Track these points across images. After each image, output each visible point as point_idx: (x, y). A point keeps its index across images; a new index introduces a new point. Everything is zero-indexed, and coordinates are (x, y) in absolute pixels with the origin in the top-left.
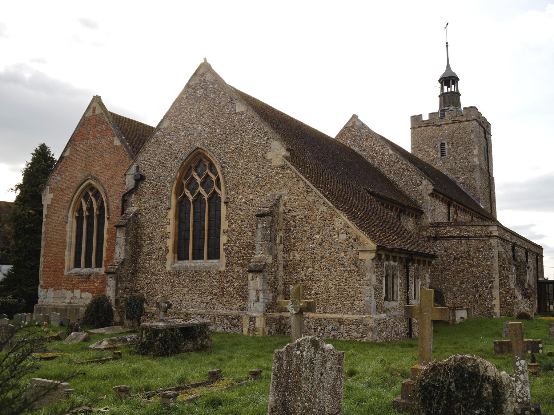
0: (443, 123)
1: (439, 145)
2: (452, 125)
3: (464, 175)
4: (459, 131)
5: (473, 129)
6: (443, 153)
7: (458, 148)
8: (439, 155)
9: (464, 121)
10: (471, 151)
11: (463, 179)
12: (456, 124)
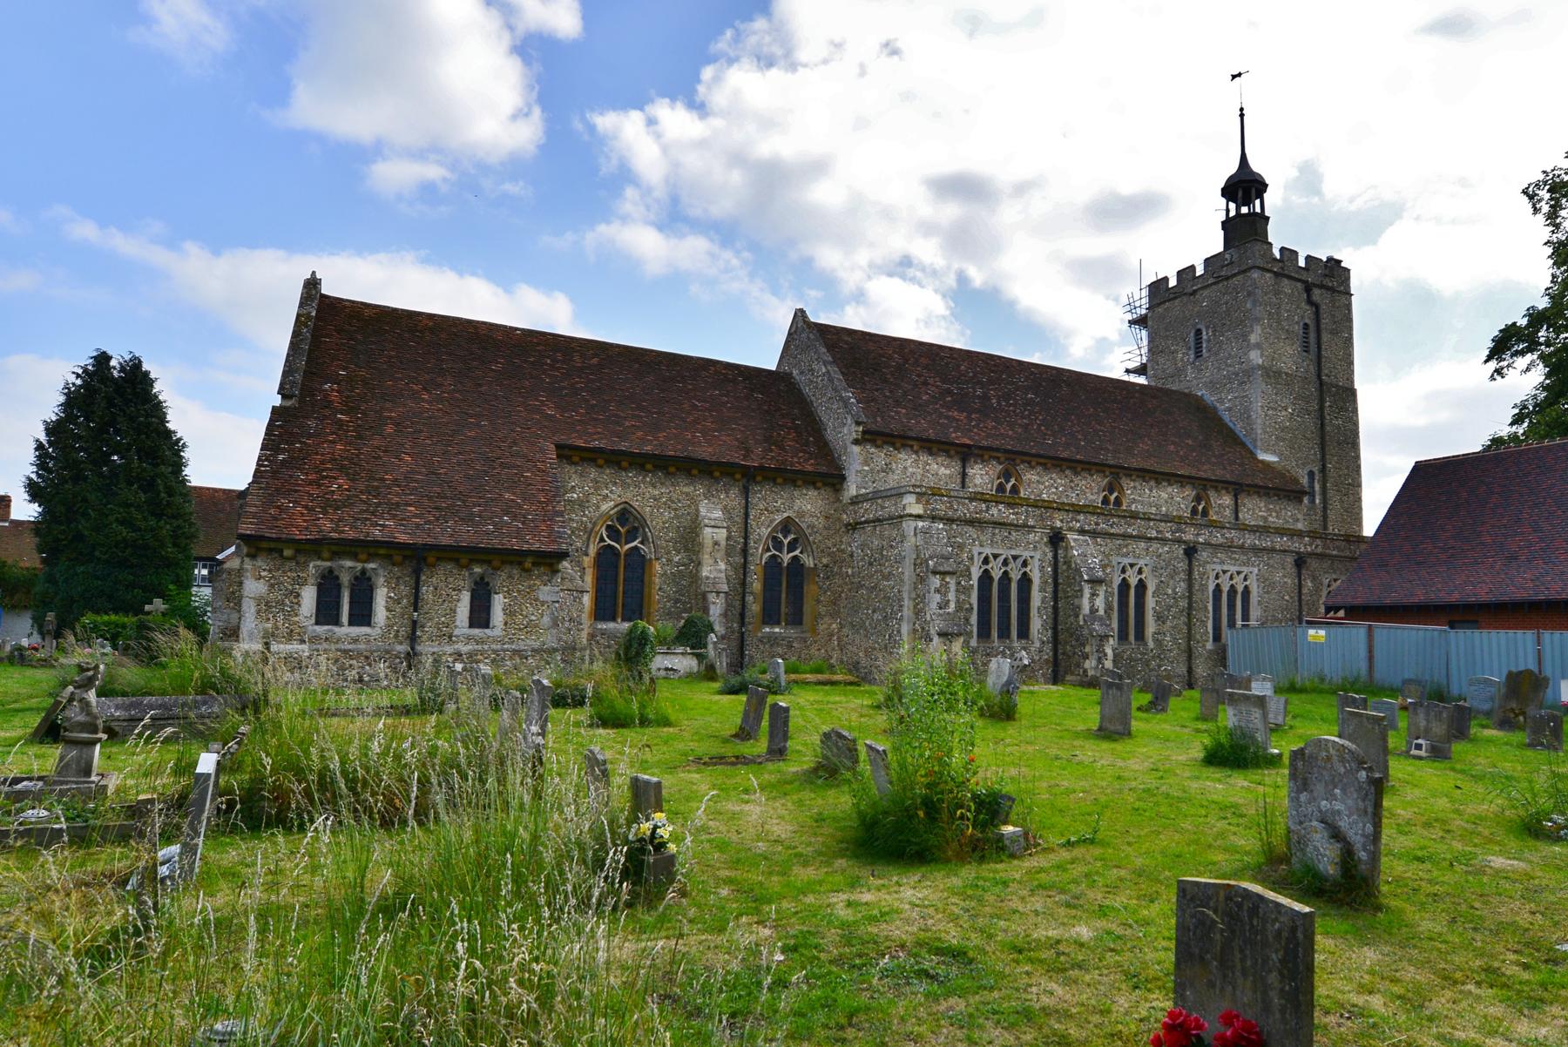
0: (1199, 286)
1: (1192, 334)
4: (1227, 297)
6: (1198, 354)
7: (1223, 335)
9: (1235, 275)
12: (1221, 285)
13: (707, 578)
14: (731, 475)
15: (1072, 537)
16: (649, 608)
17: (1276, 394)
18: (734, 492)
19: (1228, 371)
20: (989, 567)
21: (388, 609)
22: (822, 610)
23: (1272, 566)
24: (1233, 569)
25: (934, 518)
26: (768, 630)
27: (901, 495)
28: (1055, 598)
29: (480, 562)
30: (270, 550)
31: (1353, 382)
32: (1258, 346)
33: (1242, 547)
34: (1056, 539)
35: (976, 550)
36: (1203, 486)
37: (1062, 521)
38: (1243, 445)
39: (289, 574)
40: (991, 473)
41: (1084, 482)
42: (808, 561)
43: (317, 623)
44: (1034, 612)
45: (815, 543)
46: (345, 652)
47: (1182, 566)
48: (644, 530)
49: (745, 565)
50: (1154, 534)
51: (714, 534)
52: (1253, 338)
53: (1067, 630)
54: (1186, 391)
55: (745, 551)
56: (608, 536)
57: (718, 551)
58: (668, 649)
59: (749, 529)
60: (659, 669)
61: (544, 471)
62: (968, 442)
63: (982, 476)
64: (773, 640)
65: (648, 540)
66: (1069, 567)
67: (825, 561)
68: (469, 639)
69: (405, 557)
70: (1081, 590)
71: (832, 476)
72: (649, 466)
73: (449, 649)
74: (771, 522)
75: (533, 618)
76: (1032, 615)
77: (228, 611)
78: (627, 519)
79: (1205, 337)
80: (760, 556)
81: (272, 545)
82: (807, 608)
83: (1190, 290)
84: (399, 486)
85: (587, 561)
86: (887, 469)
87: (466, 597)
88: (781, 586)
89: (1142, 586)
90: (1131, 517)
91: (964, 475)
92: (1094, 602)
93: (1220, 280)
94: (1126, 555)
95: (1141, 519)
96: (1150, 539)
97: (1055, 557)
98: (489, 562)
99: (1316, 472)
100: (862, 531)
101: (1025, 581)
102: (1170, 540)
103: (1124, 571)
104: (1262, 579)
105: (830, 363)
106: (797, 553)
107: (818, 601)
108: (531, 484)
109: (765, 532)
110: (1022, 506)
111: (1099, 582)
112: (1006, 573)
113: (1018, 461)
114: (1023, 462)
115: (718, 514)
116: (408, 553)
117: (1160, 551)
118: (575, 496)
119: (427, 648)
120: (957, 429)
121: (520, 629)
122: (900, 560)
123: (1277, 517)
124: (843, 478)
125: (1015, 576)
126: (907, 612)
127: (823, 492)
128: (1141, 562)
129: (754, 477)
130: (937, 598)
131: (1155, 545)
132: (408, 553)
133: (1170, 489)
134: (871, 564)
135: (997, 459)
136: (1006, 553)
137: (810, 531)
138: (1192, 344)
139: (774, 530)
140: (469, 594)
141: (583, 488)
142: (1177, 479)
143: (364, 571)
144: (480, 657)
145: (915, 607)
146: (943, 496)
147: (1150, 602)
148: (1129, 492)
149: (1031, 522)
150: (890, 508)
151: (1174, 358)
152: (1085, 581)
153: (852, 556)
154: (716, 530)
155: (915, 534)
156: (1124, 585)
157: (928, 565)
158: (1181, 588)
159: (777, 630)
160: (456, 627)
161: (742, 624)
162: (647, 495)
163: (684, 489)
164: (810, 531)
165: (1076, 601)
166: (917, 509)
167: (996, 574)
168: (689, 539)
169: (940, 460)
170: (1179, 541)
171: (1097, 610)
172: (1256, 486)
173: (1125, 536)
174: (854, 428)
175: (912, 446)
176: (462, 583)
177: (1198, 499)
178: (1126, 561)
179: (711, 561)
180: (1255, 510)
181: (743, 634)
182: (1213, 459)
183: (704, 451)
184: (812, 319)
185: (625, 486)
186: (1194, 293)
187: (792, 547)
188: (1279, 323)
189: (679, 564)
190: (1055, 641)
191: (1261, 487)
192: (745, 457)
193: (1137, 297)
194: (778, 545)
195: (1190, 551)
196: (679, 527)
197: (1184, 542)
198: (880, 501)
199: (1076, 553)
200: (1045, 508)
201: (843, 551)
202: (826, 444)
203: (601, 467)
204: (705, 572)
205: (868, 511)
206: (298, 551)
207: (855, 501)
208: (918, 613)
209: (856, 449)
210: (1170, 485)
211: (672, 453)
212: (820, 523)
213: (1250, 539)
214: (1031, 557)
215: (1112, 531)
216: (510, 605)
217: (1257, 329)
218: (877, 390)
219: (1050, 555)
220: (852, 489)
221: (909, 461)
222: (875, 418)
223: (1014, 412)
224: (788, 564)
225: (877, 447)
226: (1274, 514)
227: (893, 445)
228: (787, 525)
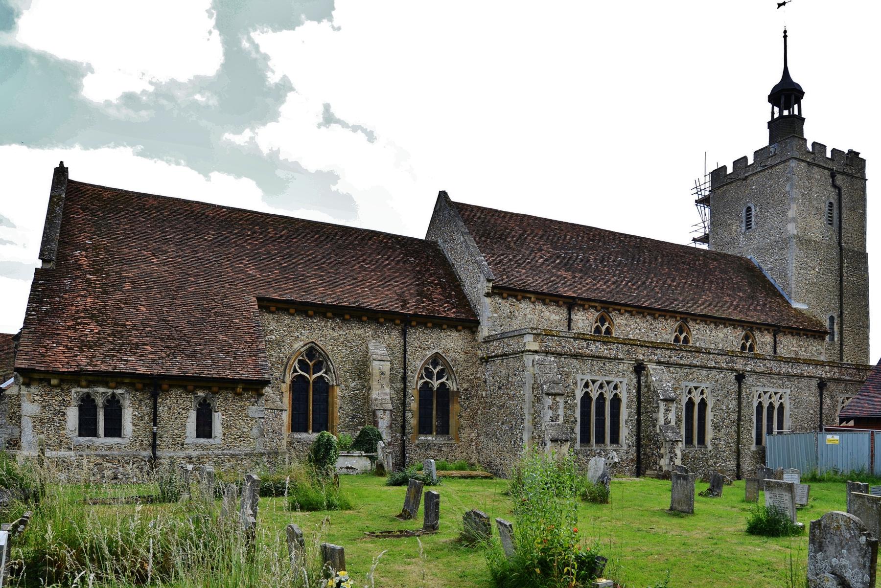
0: (750, 173)
1: (744, 211)
3: (773, 256)
4: (771, 182)
6: (748, 226)
13: (376, 399)
14: (392, 321)
15: (651, 367)
16: (333, 422)
17: (807, 257)
18: (395, 334)
20: (588, 390)
21: (134, 425)
22: (464, 423)
24: (772, 390)
25: (547, 353)
26: (423, 438)
27: (522, 335)
28: (639, 413)
29: (203, 388)
31: (865, 248)
32: (794, 220)
33: (779, 374)
34: (639, 369)
35: (579, 377)
36: (750, 327)
37: (643, 355)
38: (781, 296)
40: (590, 318)
41: (661, 325)
42: (452, 386)
43: (80, 435)
44: (622, 424)
45: (457, 372)
46: (103, 456)
47: (734, 388)
48: (327, 363)
49: (404, 390)
50: (713, 364)
51: (380, 366)
52: (791, 214)
53: (647, 437)
54: (739, 255)
55: (404, 379)
56: (299, 368)
57: (384, 378)
58: (348, 453)
59: (407, 361)
61: (249, 318)
62: (573, 295)
63: (584, 321)
64: (427, 446)
65: (330, 370)
66: (649, 390)
67: (465, 386)
68: (197, 446)
69: (145, 385)
70: (658, 407)
72: (329, 314)
73: (182, 454)
74: (424, 356)
75: (245, 430)
76: (621, 425)
77: (12, 426)
78: (314, 355)
79: (753, 213)
80: (415, 383)
82: (452, 422)
85: (285, 387)
86: (511, 315)
87: (193, 415)
88: (432, 405)
89: (703, 404)
90: (697, 352)
91: (570, 320)
94: (692, 380)
95: (703, 353)
96: (710, 368)
97: (639, 382)
98: (209, 388)
99: (836, 317)
100: (492, 363)
101: (616, 401)
102: (725, 369)
103: (690, 392)
104: (794, 399)
105: (467, 233)
106: (444, 380)
107: (460, 416)
109: (419, 364)
110: (614, 343)
111: (672, 400)
112: (601, 394)
113: (611, 309)
114: (614, 310)
115: (383, 351)
117: (717, 377)
118: (274, 337)
119: (165, 454)
120: (565, 285)
121: (235, 439)
122: (521, 385)
123: (806, 351)
124: (478, 323)
125: (609, 396)
126: (527, 424)
127: (462, 333)
128: (703, 386)
129: (410, 322)
130: (550, 413)
131: (714, 373)
133: (725, 330)
134: (500, 388)
135: (595, 308)
136: (602, 379)
137: (453, 363)
138: (744, 219)
139: (426, 363)
140: (195, 412)
141: (279, 331)
142: (731, 323)
143: (113, 395)
144: (206, 460)
145: (533, 420)
146: (554, 336)
147: (709, 416)
148: (694, 333)
149: (620, 356)
150: (513, 345)
151: (730, 230)
152: (661, 400)
153: (485, 382)
154: (382, 363)
155: (533, 366)
156: (690, 403)
157: (542, 389)
158: (733, 404)
160: (186, 437)
161: (404, 433)
163: (357, 332)
164: (453, 363)
166: (535, 346)
167: (594, 395)
168: (362, 370)
169: (551, 308)
170: (732, 370)
171: (670, 422)
172: (790, 328)
173: (691, 366)
174: (486, 284)
175: (530, 298)
177: (746, 338)
178: (692, 385)
179: (379, 387)
180: (789, 346)
181: (404, 441)
182: (758, 308)
183: (371, 303)
186: (746, 178)
187: (440, 375)
188: (810, 202)
189: (354, 389)
191: (794, 328)
192: (403, 307)
193: (702, 182)
194: (429, 374)
195: (740, 378)
196: (353, 361)
197: (736, 370)
198: (506, 340)
199: (654, 379)
200: (631, 345)
201: (478, 378)
202: (465, 297)
203: (292, 315)
204: (374, 394)
205: (497, 348)
207: (487, 340)
208: (536, 424)
209: (488, 300)
210: (725, 327)
211: (346, 304)
212: (461, 357)
213: (785, 368)
214: (621, 382)
216: (227, 420)
217: (794, 207)
218: (503, 255)
220: (484, 331)
221: (528, 310)
222: (501, 276)
223: (608, 271)
224: (437, 388)
225: (503, 298)
226: (803, 349)
227: (516, 297)
228: (435, 360)
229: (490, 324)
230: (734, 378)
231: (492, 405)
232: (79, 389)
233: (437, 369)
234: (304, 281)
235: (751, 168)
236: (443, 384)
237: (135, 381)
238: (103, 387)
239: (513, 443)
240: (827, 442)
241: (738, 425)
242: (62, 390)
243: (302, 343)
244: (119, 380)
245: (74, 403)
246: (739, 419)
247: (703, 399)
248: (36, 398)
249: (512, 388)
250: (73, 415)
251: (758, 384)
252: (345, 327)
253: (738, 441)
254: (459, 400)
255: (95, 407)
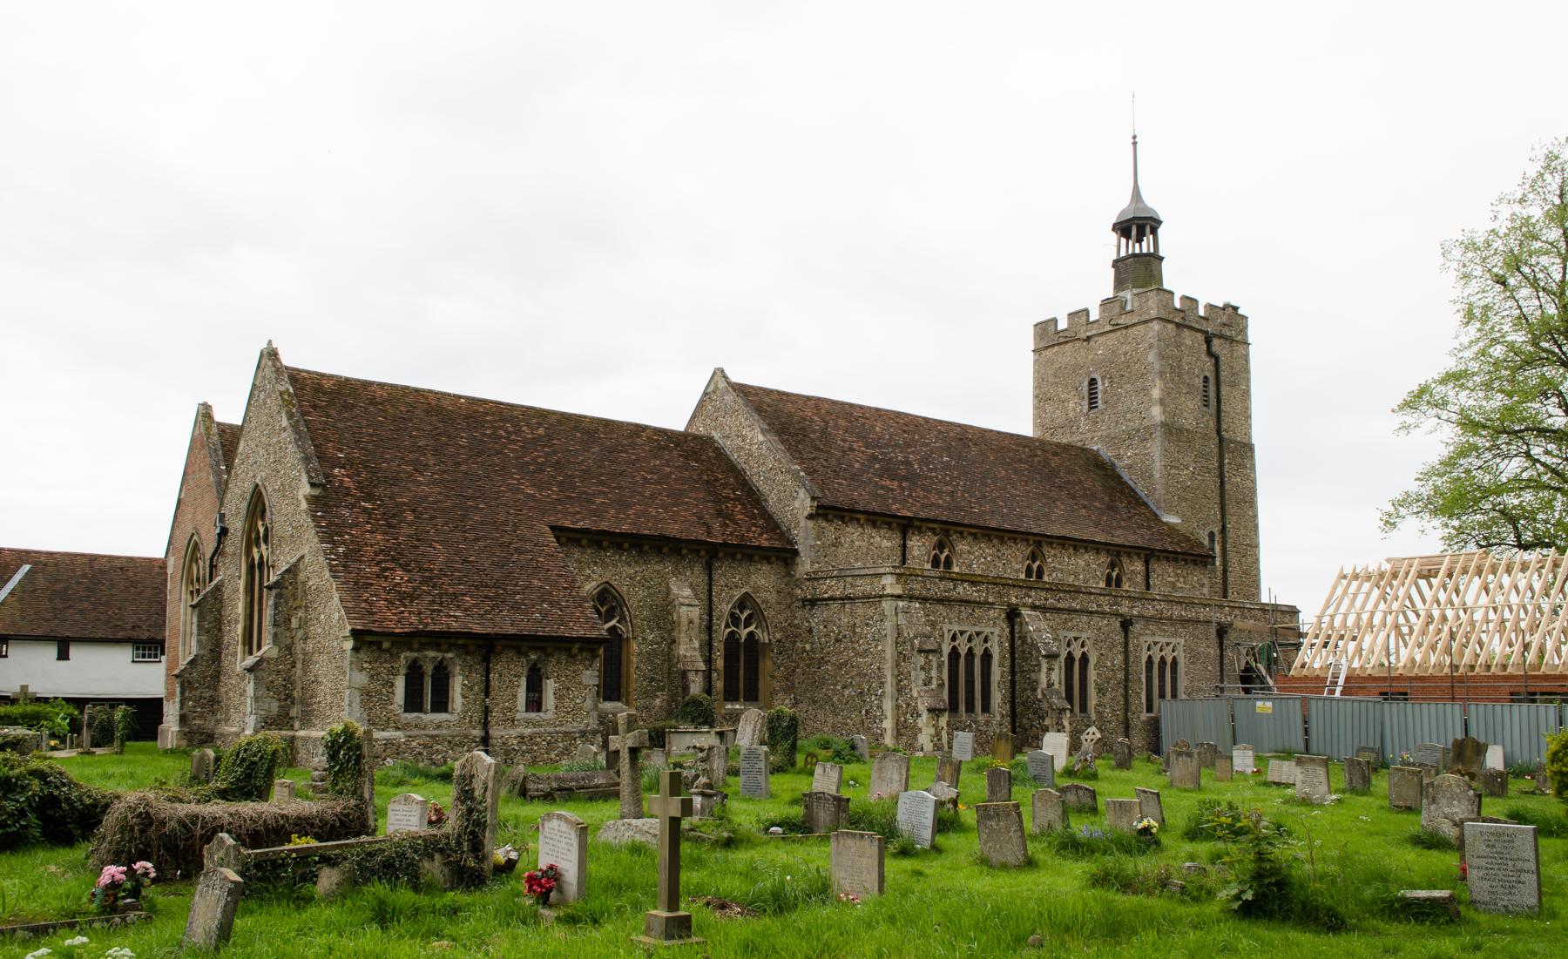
0: (1094, 332)
2: (1111, 335)
4: (1125, 348)
5: (1152, 340)
6: (1092, 404)
8: (1086, 407)
9: (1134, 325)
10: (1145, 391)
11: (1129, 457)
12: (1119, 333)
15: (1025, 612)
17: (1178, 452)
18: (698, 568)
19: (1127, 426)
20: (956, 643)
21: (464, 697)
22: (777, 685)
23: (1197, 637)
24: (1163, 640)
25: (911, 598)
28: (1013, 673)
30: (371, 643)
31: (1250, 437)
33: (1170, 619)
34: (1012, 615)
35: (946, 627)
37: (1016, 597)
38: (1145, 504)
39: (385, 665)
40: (927, 544)
41: (1009, 551)
42: (763, 637)
43: (405, 711)
46: (433, 737)
47: (1119, 638)
50: (1095, 608)
51: (689, 612)
53: (1023, 703)
54: (1079, 444)
60: (689, 748)
62: (909, 514)
63: (920, 547)
65: (625, 618)
66: (1024, 642)
67: (778, 636)
68: (528, 722)
70: (1039, 665)
71: (786, 550)
72: (626, 545)
73: (514, 732)
75: (578, 701)
76: (992, 689)
77: (269, 699)
79: (1100, 387)
80: (722, 632)
81: (374, 638)
82: (764, 684)
83: (1083, 336)
84: (446, 576)
86: (836, 544)
87: (523, 682)
88: (738, 661)
89: (1084, 659)
90: (1076, 592)
91: (904, 546)
92: (1050, 677)
93: (1117, 328)
94: (1071, 629)
95: (1083, 593)
96: (1092, 612)
97: (1012, 632)
98: (543, 649)
100: (823, 608)
101: (987, 656)
102: (1109, 613)
106: (752, 628)
107: (773, 677)
108: (548, 570)
110: (983, 583)
111: (1055, 656)
112: (970, 649)
113: (952, 532)
114: (956, 532)
116: (481, 642)
119: (496, 732)
120: (895, 500)
121: (568, 713)
122: (877, 639)
123: (1185, 583)
124: (796, 553)
125: (978, 652)
127: (774, 566)
128: (1084, 636)
130: (923, 675)
131: (1096, 619)
132: (481, 642)
133: (1086, 556)
135: (933, 530)
139: (733, 607)
142: (1094, 546)
144: (538, 740)
145: (898, 684)
147: (1092, 675)
148: (1050, 560)
149: (991, 600)
151: (1065, 408)
153: (810, 631)
156: (1070, 658)
157: (912, 645)
159: (738, 707)
160: (517, 711)
162: (624, 574)
163: (654, 568)
165: (1033, 676)
166: (898, 590)
167: (963, 651)
168: (663, 616)
169: (882, 532)
170: (1117, 614)
171: (1053, 684)
172: (1166, 551)
173: (1070, 611)
175: (858, 520)
176: (520, 670)
177: (1112, 566)
178: (1071, 635)
179: (687, 640)
180: (1165, 576)
182: (1123, 524)
184: (734, 378)
185: (605, 565)
186: (1088, 339)
187: (748, 623)
188: (1180, 377)
189: (653, 643)
190: (1013, 715)
191: (1171, 552)
192: (709, 533)
195: (1126, 624)
197: (1121, 615)
198: (849, 579)
199: (1031, 629)
200: (1002, 585)
201: (797, 627)
203: (583, 547)
206: (393, 643)
208: (900, 690)
210: (1087, 551)
211: (647, 532)
213: (1177, 611)
214: (992, 633)
215: (1059, 605)
219: (1007, 630)
220: (805, 565)
223: (937, 478)
226: (1182, 580)
227: (842, 519)
228: (742, 603)
229: (813, 554)
230: (1119, 625)
231: (822, 661)
232: (408, 654)
233: (745, 615)
234: (589, 501)
235: (1095, 326)
236: (751, 634)
237: (469, 642)
238: (433, 650)
239: (863, 712)
240: (1258, 710)
241: (1126, 687)
242: (391, 654)
243: (594, 584)
244: (452, 641)
245: (403, 671)
246: (1126, 679)
247: (1084, 654)
248: (365, 665)
249: (861, 641)
250: (400, 684)
251: (1147, 631)
252: (641, 562)
253: (1126, 709)
254: (771, 654)
255: (422, 675)
